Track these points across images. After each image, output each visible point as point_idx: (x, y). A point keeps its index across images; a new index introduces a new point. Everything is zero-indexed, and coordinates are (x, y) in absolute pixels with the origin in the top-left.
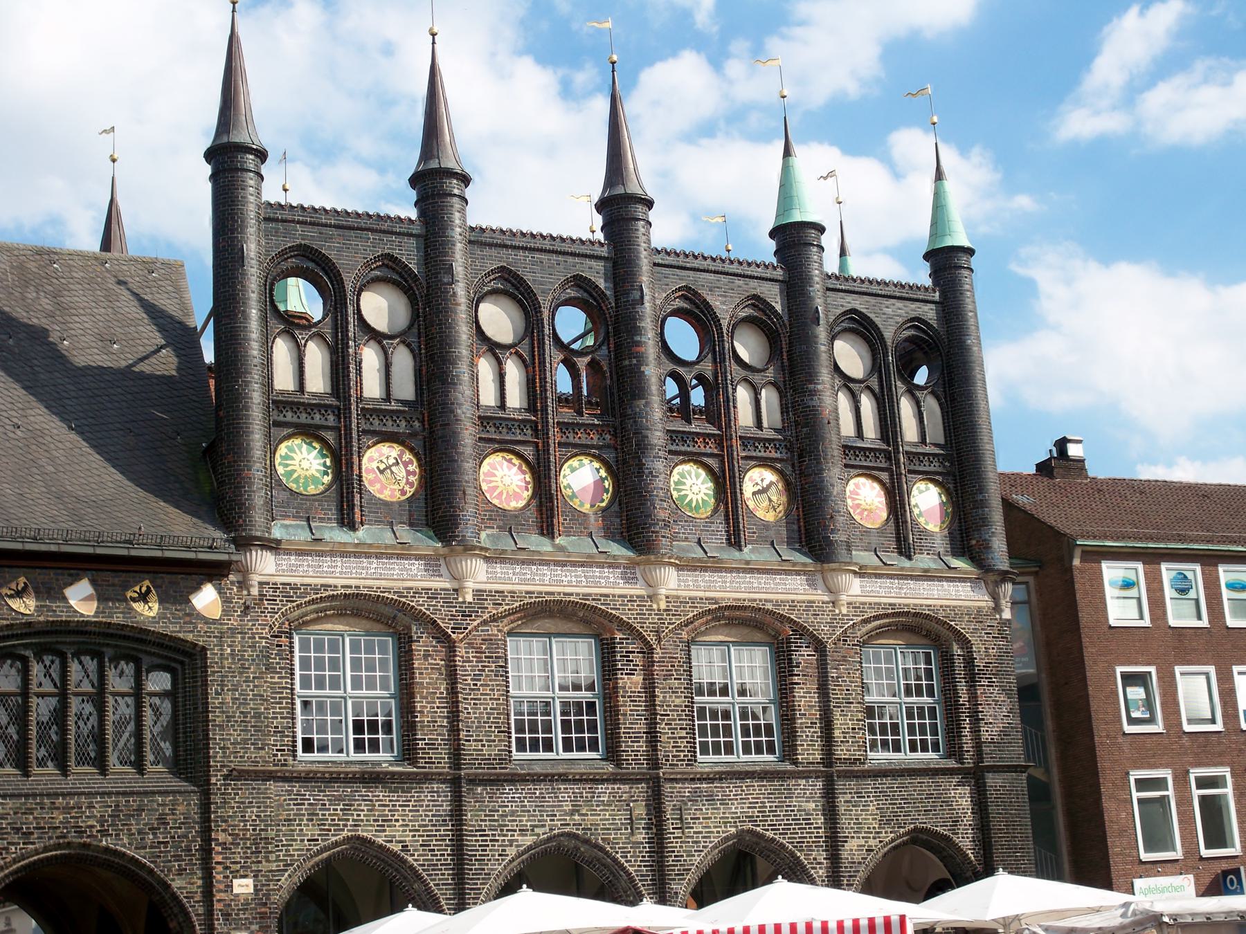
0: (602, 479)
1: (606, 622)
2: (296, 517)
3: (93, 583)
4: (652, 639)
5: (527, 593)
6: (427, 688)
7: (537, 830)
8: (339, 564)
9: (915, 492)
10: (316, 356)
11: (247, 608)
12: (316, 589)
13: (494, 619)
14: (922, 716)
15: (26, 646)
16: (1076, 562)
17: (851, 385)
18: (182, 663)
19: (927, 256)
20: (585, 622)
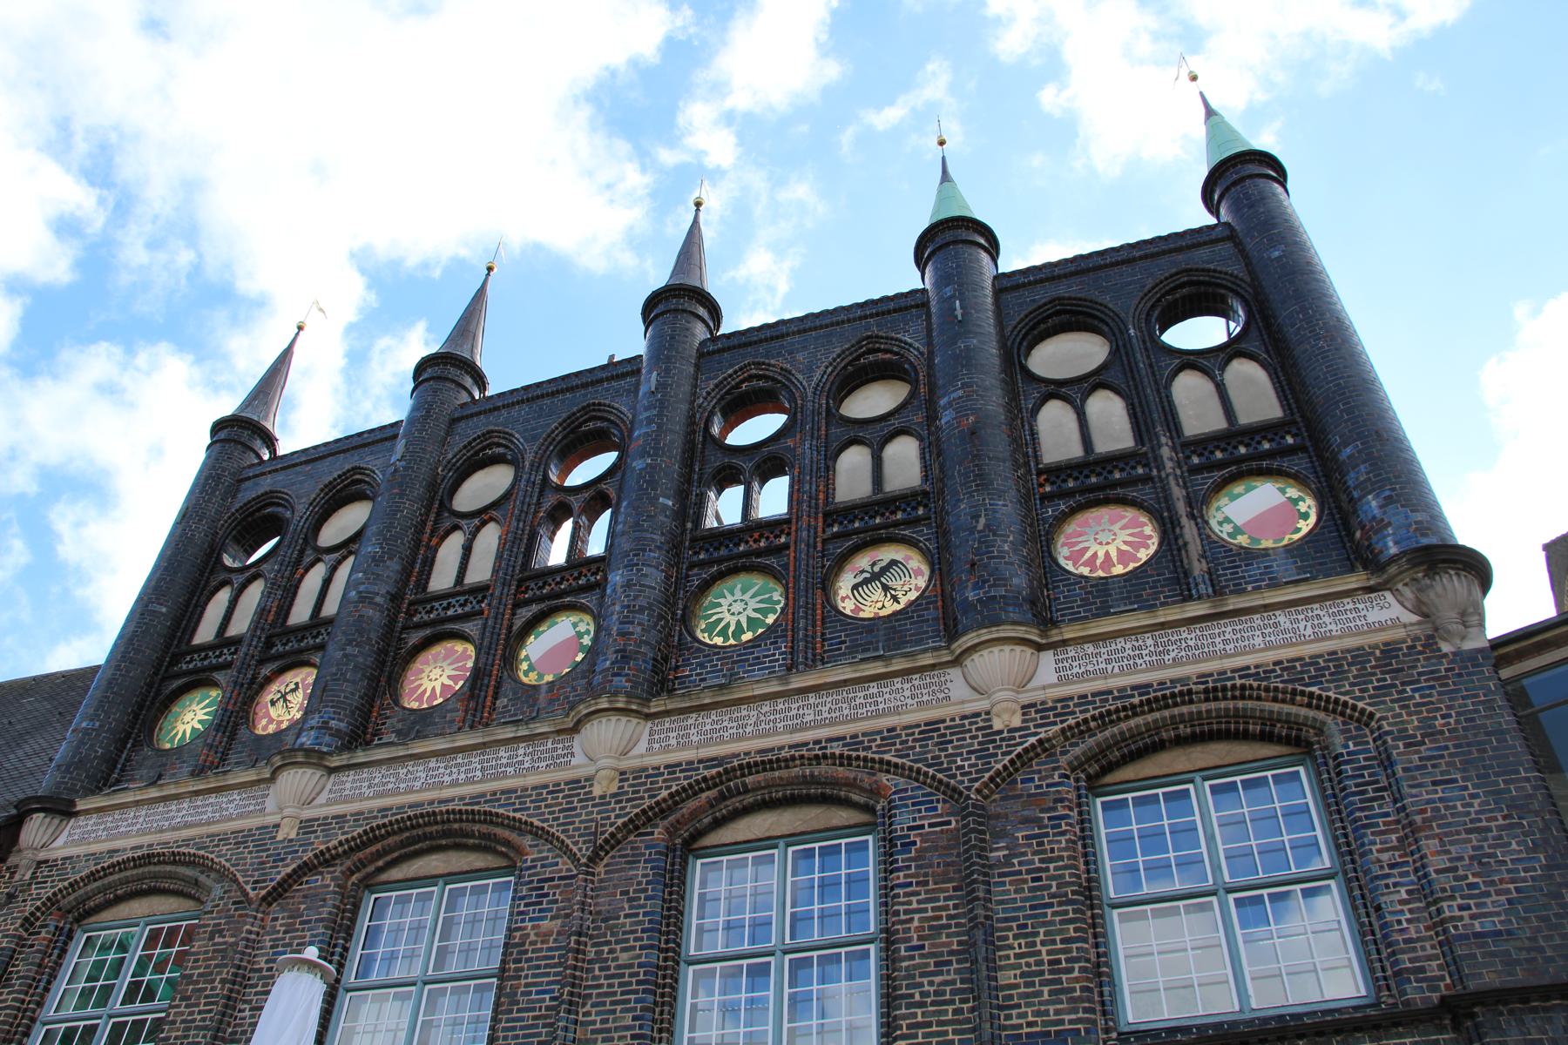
0: (580, 635)
13: (325, 860)
20: (487, 845)
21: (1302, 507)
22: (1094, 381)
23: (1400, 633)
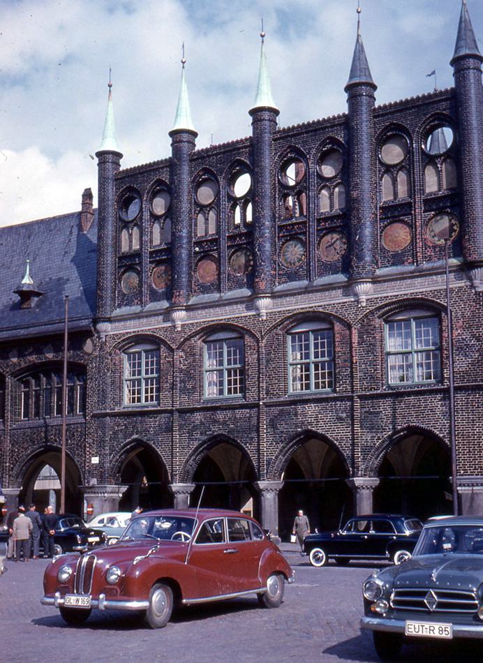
5: (203, 322)
7: (207, 433)
21: (455, 228)
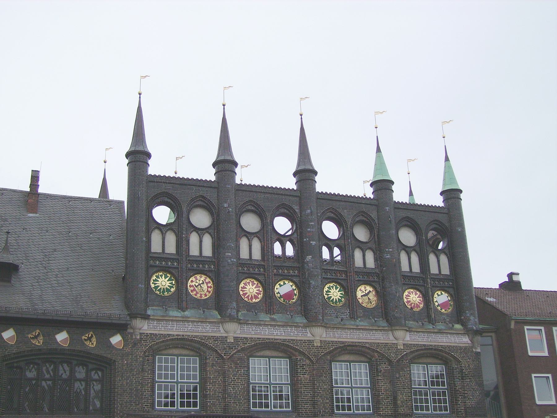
0: (294, 290)
1: (294, 352)
2: (157, 306)
3: (68, 332)
4: (314, 359)
5: (258, 338)
6: (213, 379)
8: (175, 326)
9: (436, 295)
10: (171, 239)
11: (135, 344)
12: (165, 336)
13: (243, 349)
14: (439, 395)
15: (39, 359)
16: (512, 326)
17: (407, 249)
18: (106, 367)
19: (442, 194)
22: (413, 249)
23: (467, 345)
